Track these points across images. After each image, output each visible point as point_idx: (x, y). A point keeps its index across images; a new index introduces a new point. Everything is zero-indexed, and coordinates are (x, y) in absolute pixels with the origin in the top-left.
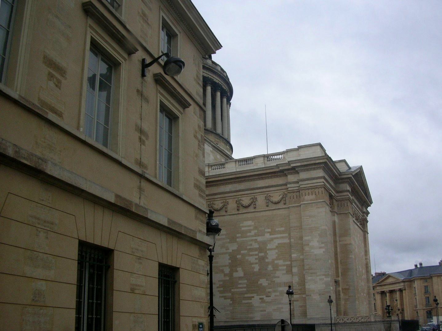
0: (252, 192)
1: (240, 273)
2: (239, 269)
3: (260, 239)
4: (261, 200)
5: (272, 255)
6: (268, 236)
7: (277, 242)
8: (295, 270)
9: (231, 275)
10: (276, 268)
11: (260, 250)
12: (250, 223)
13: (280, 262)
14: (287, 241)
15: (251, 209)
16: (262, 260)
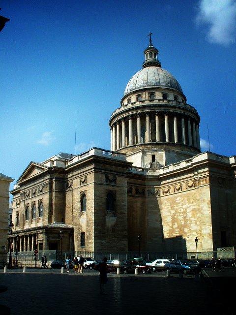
0: (180, 181)
1: (176, 226)
2: (176, 223)
3: (184, 207)
4: (184, 185)
5: (189, 215)
6: (187, 205)
7: (191, 208)
8: (198, 223)
9: (172, 227)
10: (191, 221)
11: (184, 213)
12: (179, 198)
13: (193, 219)
14: (195, 207)
15: (180, 191)
16: (185, 218)
